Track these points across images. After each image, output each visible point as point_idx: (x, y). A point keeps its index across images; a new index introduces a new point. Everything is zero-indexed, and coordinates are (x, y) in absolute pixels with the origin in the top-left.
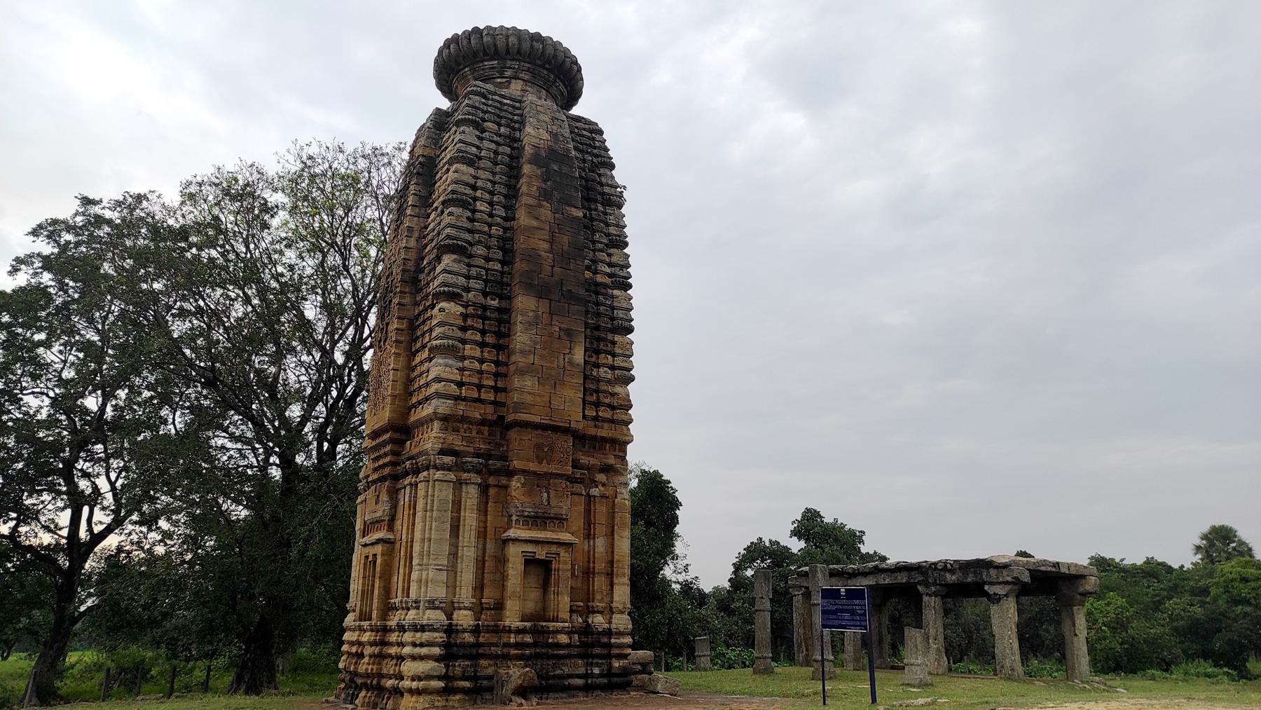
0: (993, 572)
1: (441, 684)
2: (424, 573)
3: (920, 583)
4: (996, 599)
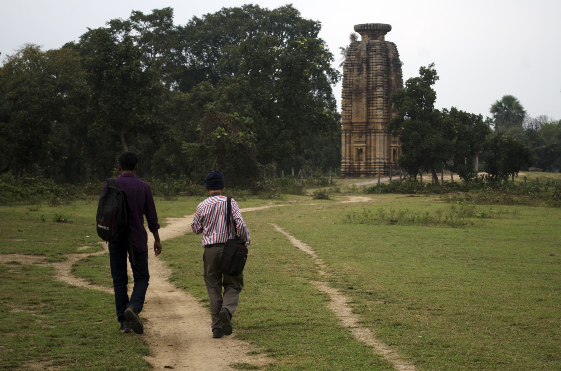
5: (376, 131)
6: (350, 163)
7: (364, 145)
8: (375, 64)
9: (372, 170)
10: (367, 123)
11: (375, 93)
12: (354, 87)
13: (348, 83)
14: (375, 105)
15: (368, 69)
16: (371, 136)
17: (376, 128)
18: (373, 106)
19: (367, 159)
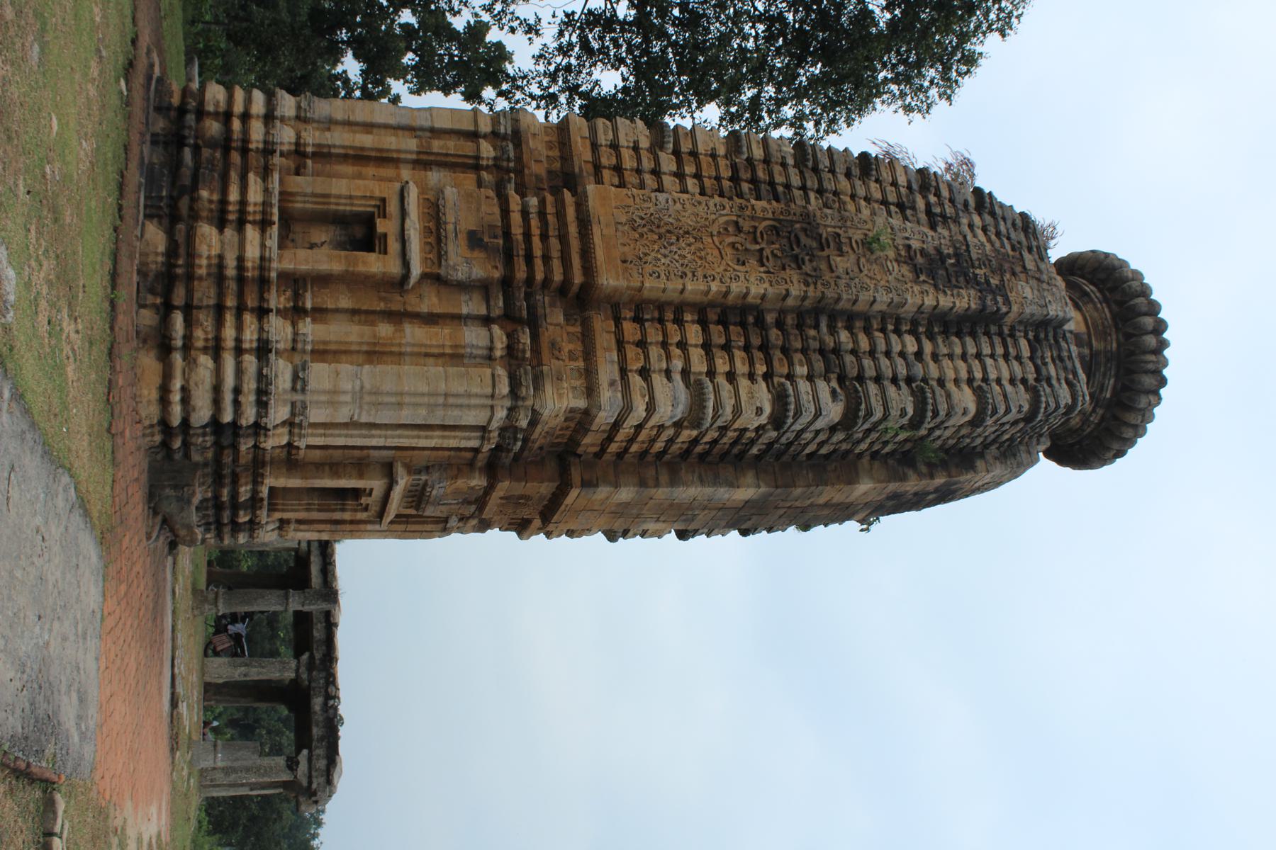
0: (322, 764)
1: (176, 421)
2: (348, 398)
3: (312, 657)
4: (292, 764)
5: (522, 368)
6: (268, 150)
7: (416, 270)
8: (978, 375)
9: (206, 321)
10: (581, 300)
11: (801, 370)
12: (828, 222)
13: (829, 185)
14: (722, 366)
15: (945, 325)
16: (486, 321)
17: (550, 365)
18: (707, 346)
19: (295, 282)
